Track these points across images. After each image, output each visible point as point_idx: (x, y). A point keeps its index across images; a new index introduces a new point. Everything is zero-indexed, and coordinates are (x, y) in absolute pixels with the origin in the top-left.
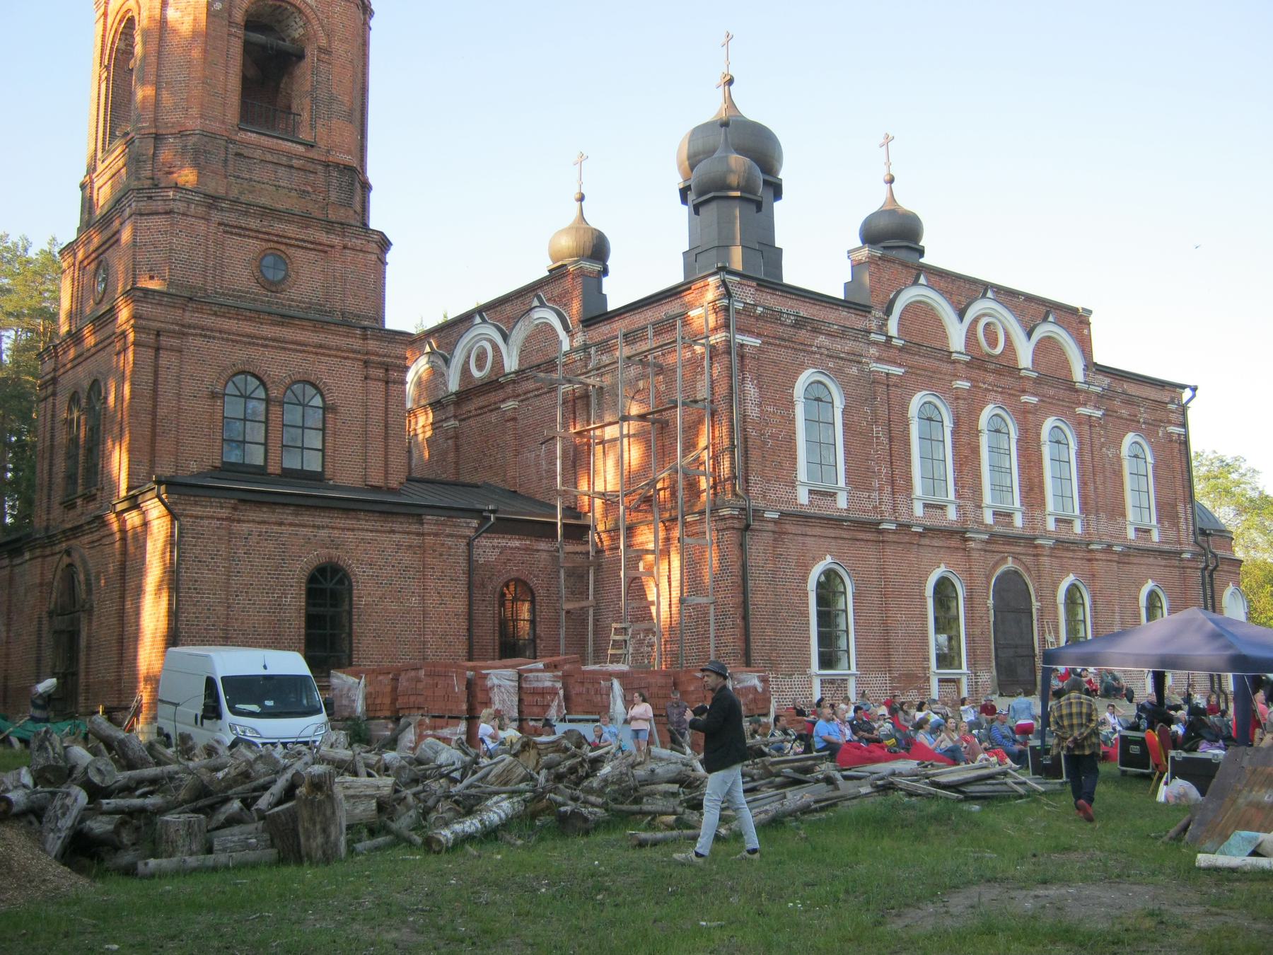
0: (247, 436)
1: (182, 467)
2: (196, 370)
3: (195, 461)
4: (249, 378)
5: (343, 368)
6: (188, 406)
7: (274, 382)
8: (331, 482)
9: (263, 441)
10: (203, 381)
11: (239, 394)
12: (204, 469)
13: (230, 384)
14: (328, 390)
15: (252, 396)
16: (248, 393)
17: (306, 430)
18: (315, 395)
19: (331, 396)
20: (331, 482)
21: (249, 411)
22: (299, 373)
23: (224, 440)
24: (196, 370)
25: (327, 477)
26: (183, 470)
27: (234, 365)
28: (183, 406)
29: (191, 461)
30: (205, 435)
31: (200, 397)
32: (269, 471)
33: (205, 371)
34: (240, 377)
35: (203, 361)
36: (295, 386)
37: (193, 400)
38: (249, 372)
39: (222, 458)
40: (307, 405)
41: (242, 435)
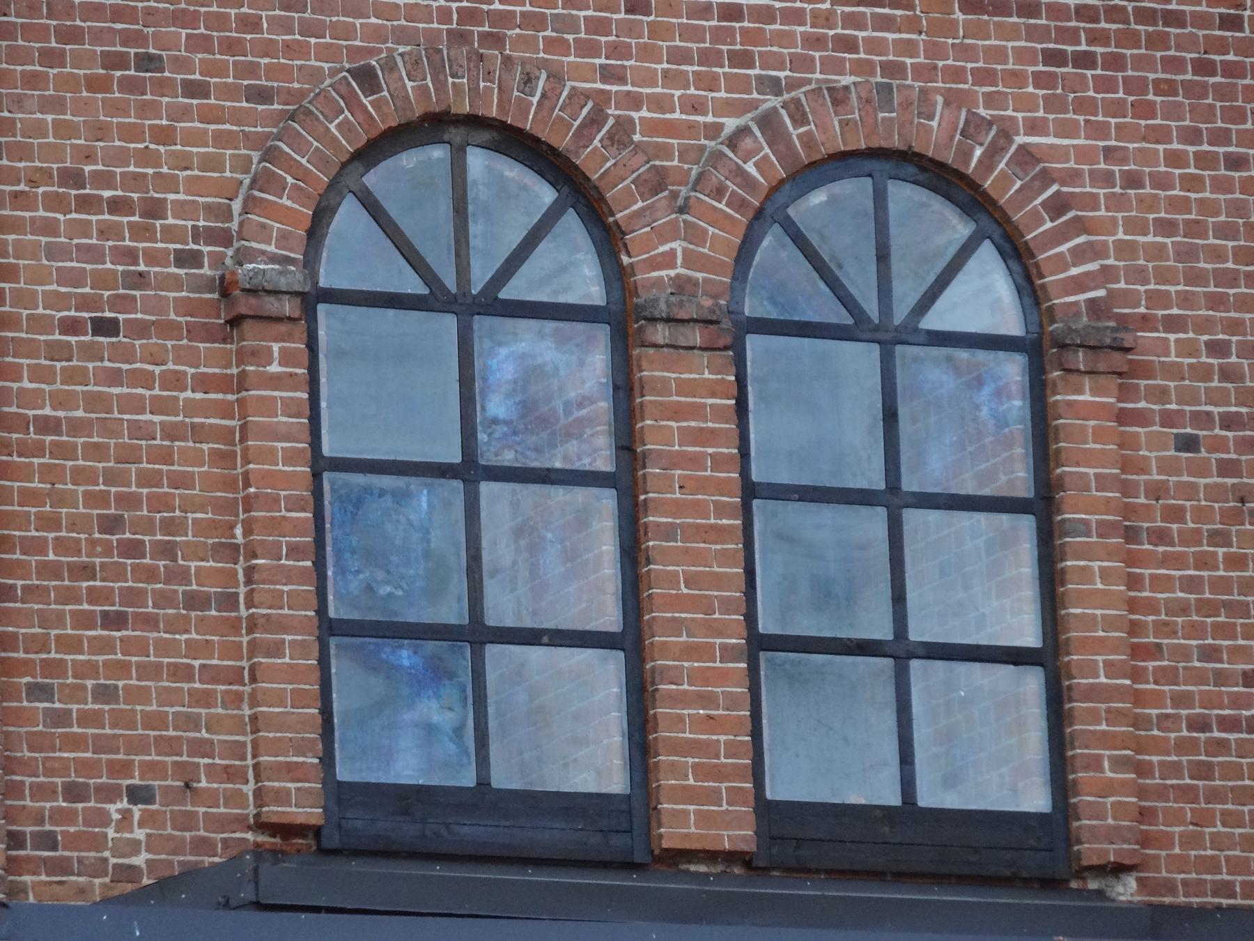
0: (491, 588)
1: (48, 841)
2: (100, 132)
3: (136, 795)
4: (478, 161)
5: (1156, 41)
6: (60, 401)
7: (657, 182)
8: (1126, 890)
9: (609, 618)
10: (154, 210)
11: (413, 285)
12: (202, 846)
13: (349, 216)
14: (1057, 206)
15: (512, 291)
16: (480, 277)
17: (913, 519)
18: (966, 251)
19: (1079, 255)
20: (1126, 890)
21: (496, 406)
22: (839, 97)
23: (328, 628)
24: (100, 132)
25: (1091, 850)
26: (62, 867)
27: (367, 78)
28: (32, 399)
29: (109, 793)
30: (196, 601)
31: (141, 330)
32: (671, 835)
33: (163, 135)
34: (409, 160)
35: (147, 62)
36: (818, 198)
37: (91, 353)
38: (474, 122)
39: (328, 760)
40: (910, 334)
41: (459, 584)
